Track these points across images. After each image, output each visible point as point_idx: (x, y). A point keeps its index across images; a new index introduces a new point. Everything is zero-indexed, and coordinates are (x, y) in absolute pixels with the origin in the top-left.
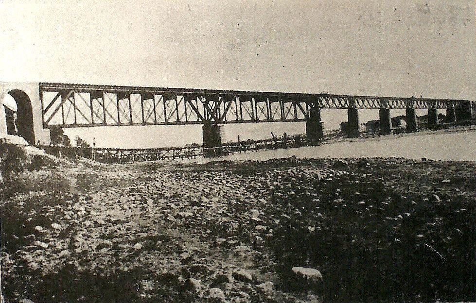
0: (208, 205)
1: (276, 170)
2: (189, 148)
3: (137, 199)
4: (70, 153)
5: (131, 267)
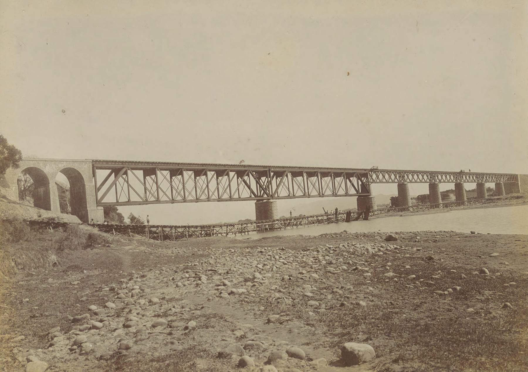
0: (262, 282)
1: (328, 245)
2: (419, 234)
3: (191, 276)
4: (122, 229)
5: (186, 346)
